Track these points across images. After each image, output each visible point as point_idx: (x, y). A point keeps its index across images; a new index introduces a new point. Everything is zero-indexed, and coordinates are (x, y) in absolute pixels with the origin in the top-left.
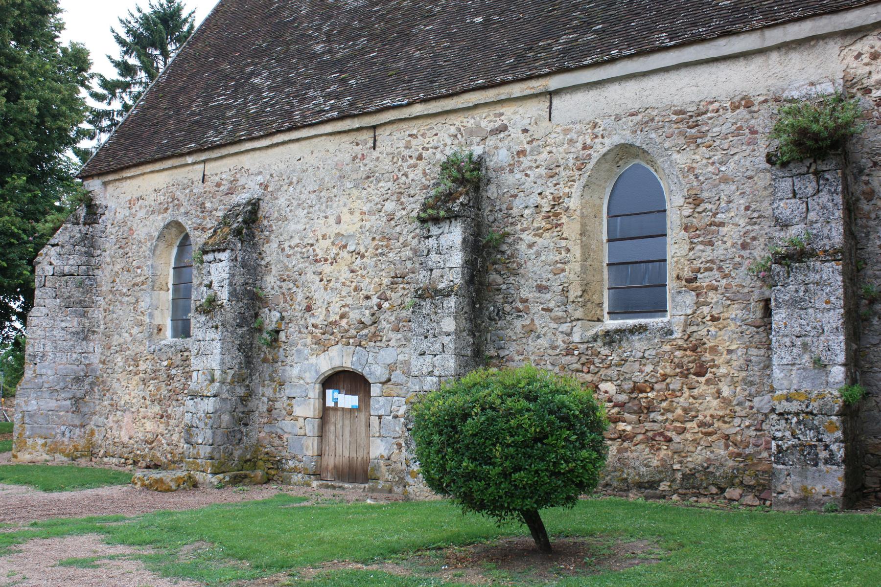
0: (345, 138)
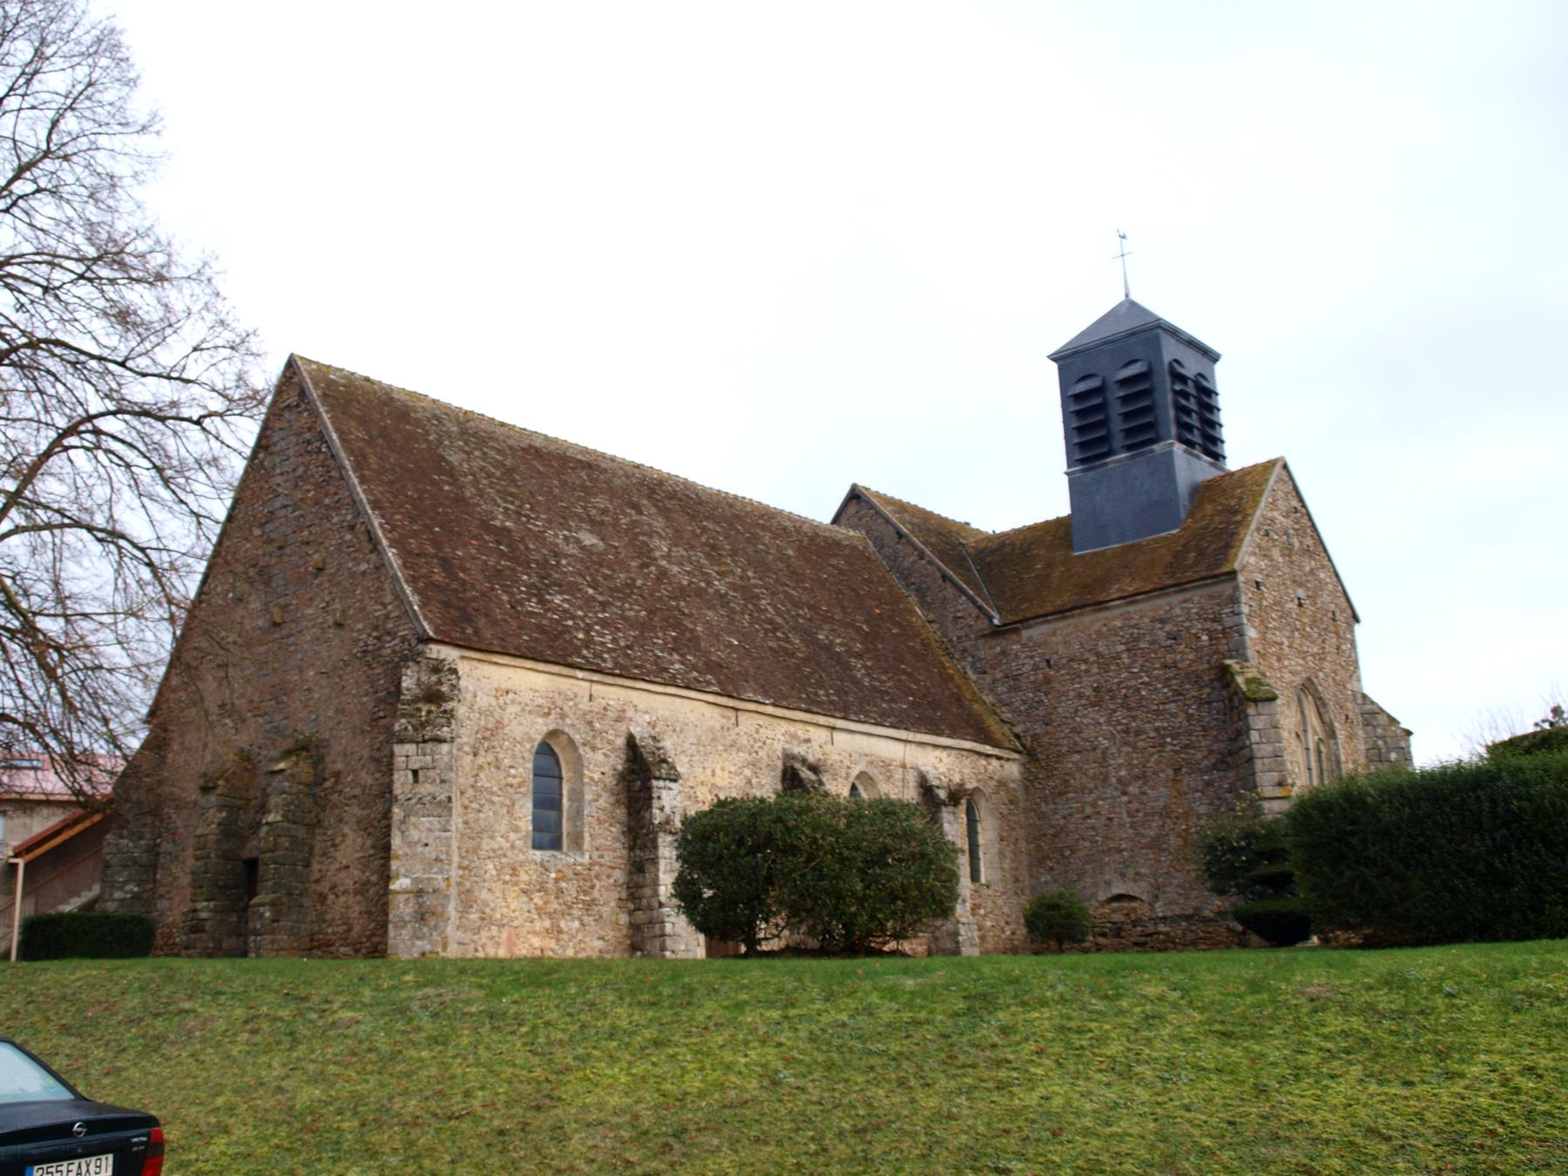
0: (717, 710)
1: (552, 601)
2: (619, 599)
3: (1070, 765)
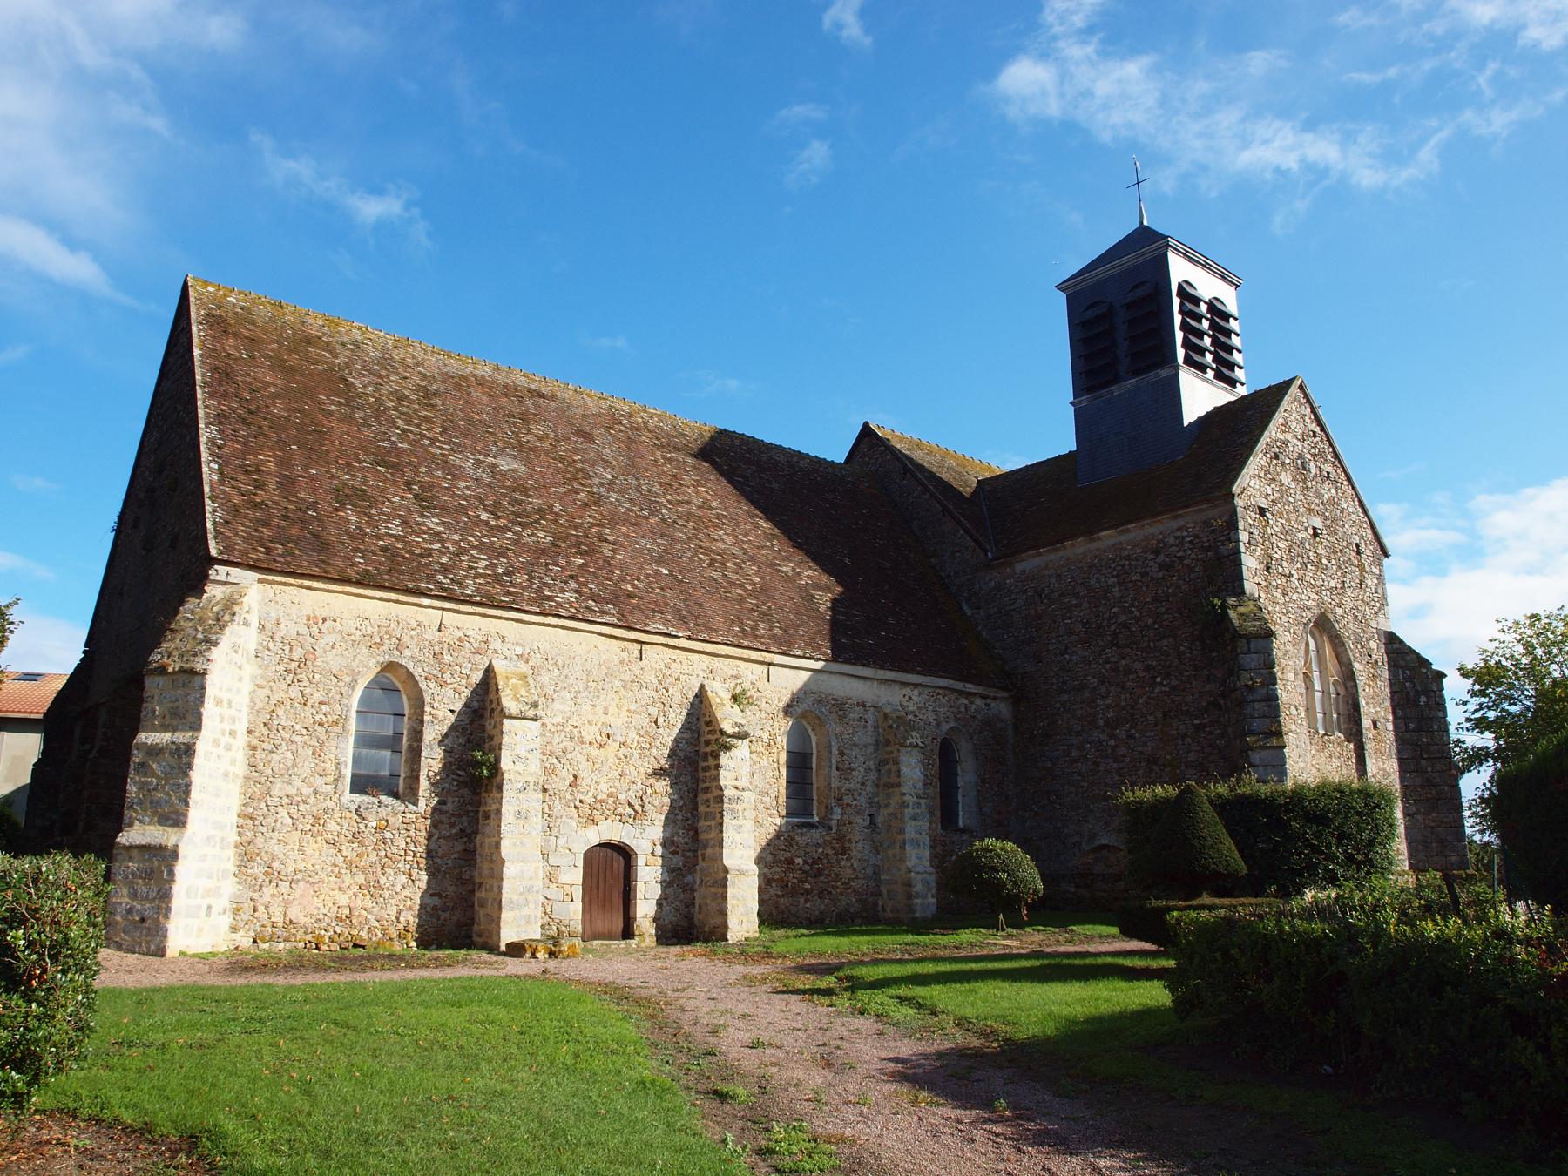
1: (424, 524)
2: (520, 524)
3: (1058, 705)
